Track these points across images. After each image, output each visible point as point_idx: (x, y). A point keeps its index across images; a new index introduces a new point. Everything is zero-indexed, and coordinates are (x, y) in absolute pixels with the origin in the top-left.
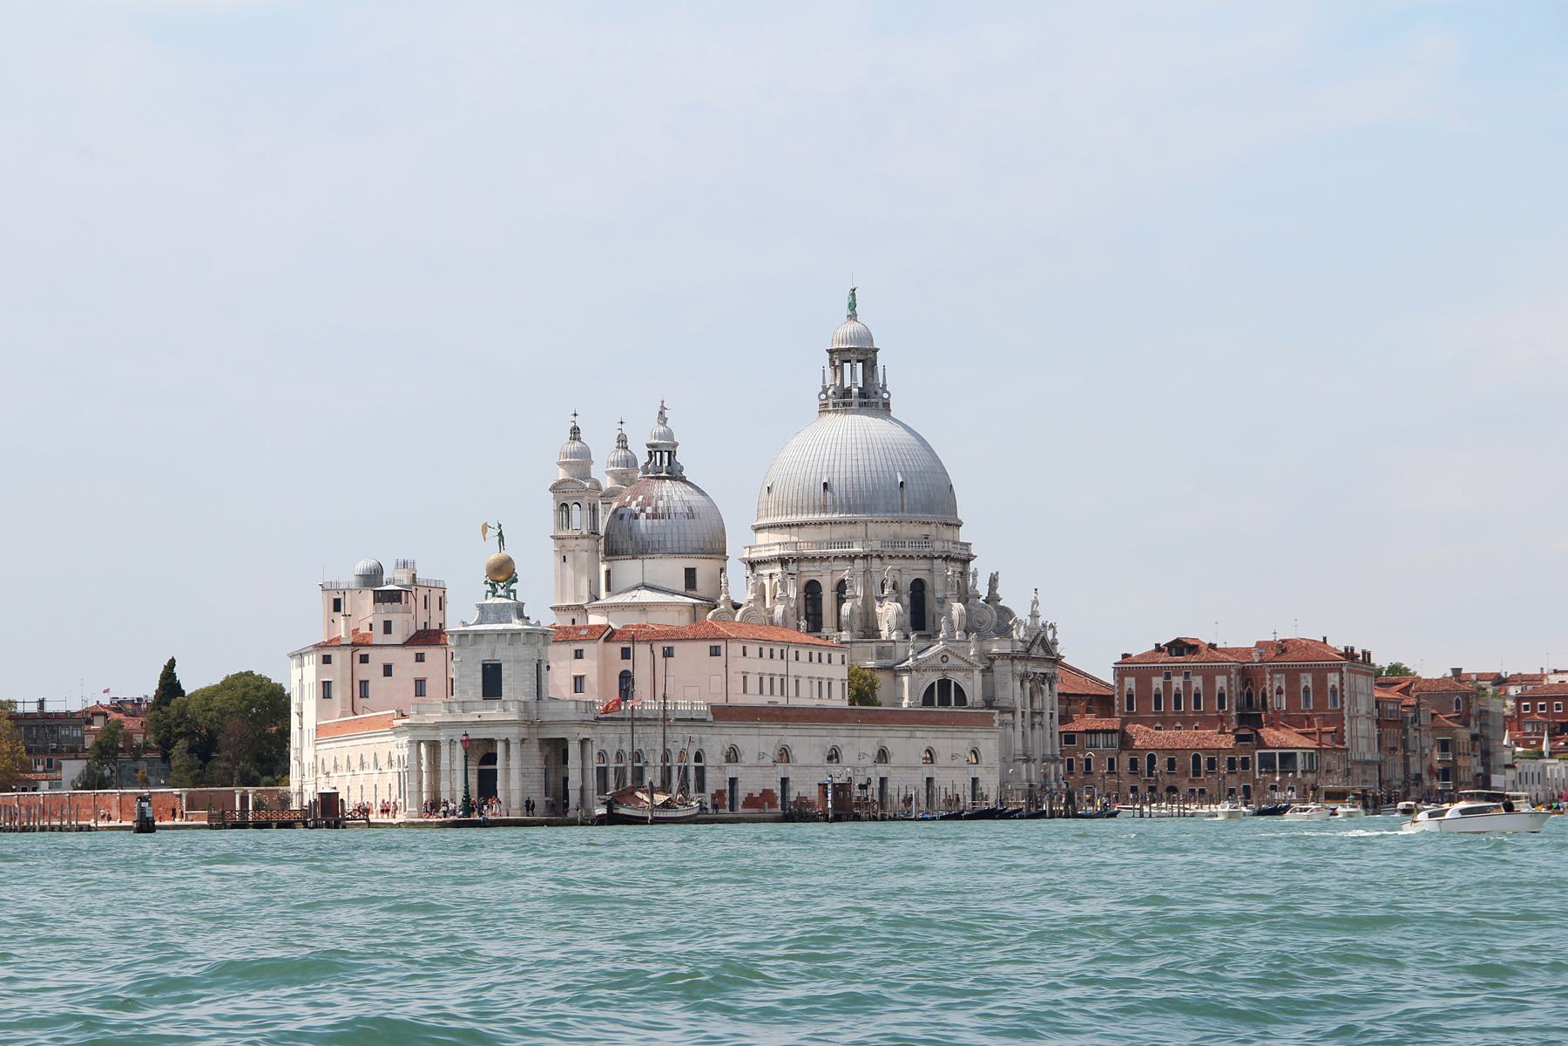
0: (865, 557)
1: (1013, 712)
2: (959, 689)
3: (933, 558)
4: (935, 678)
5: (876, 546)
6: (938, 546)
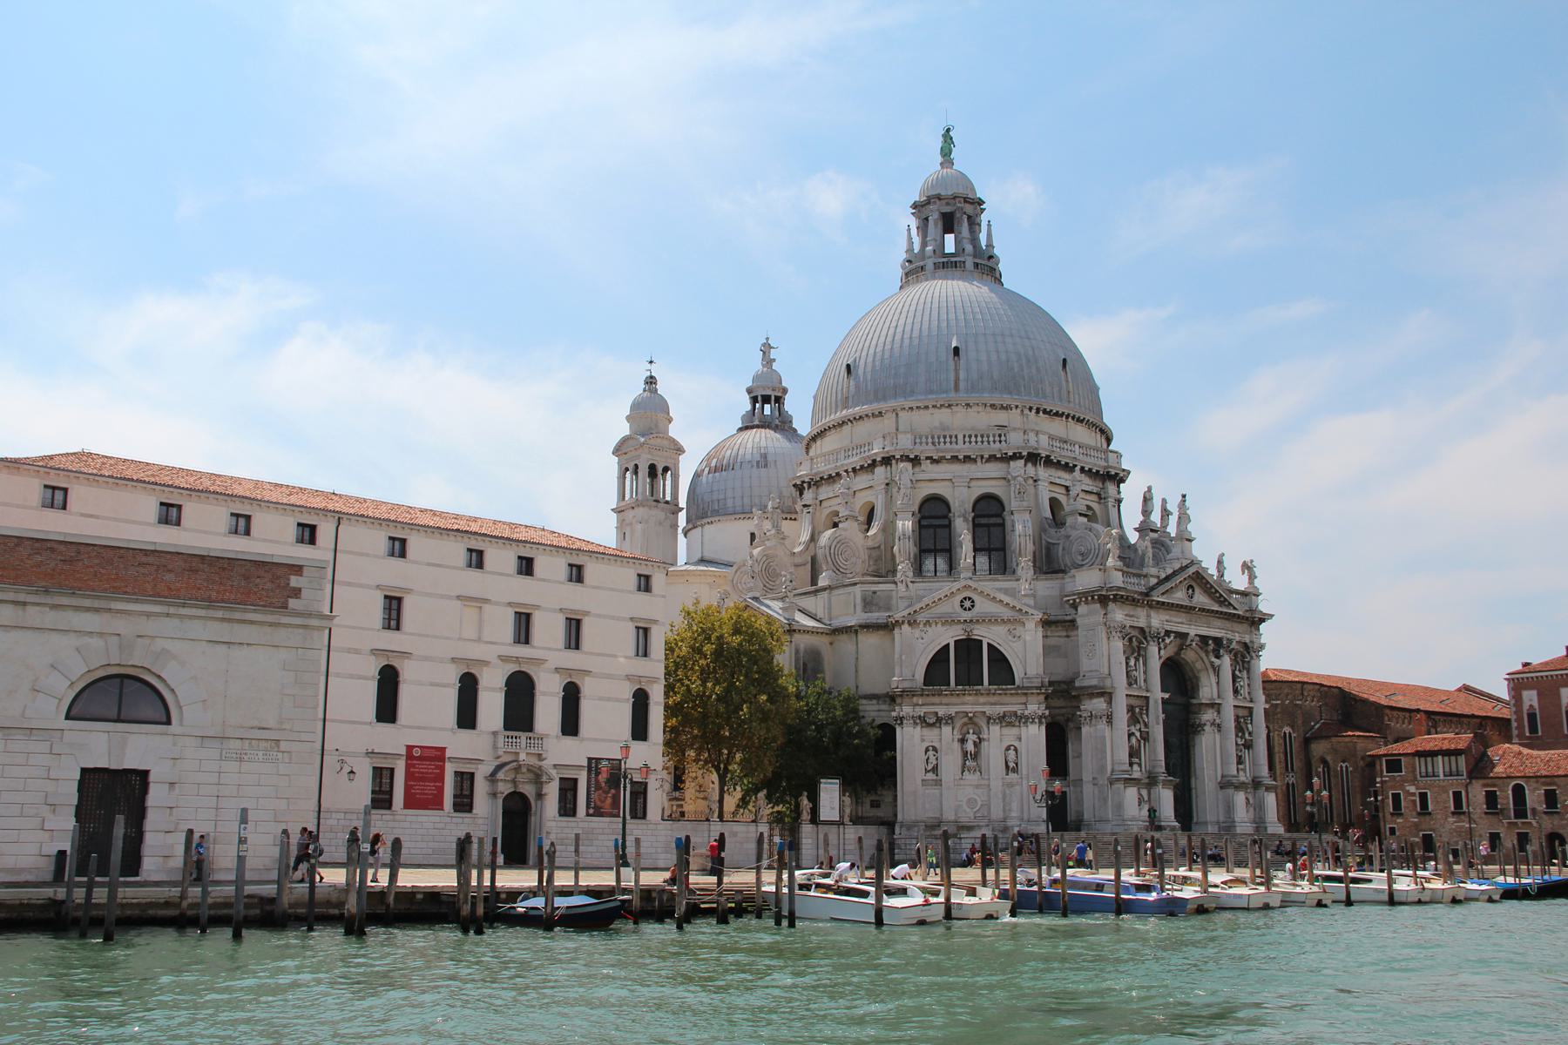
0: (887, 461)
1: (1108, 695)
2: (998, 658)
3: (1007, 459)
4: (948, 636)
5: (905, 443)
6: (1015, 441)
